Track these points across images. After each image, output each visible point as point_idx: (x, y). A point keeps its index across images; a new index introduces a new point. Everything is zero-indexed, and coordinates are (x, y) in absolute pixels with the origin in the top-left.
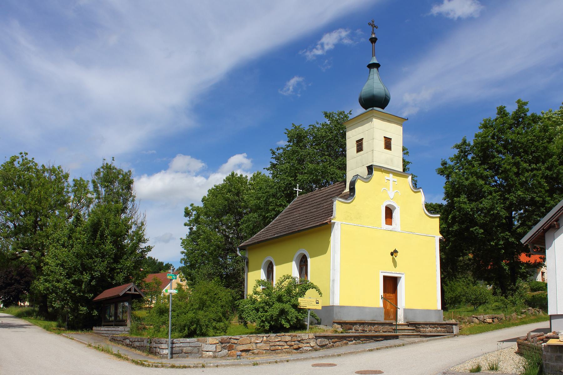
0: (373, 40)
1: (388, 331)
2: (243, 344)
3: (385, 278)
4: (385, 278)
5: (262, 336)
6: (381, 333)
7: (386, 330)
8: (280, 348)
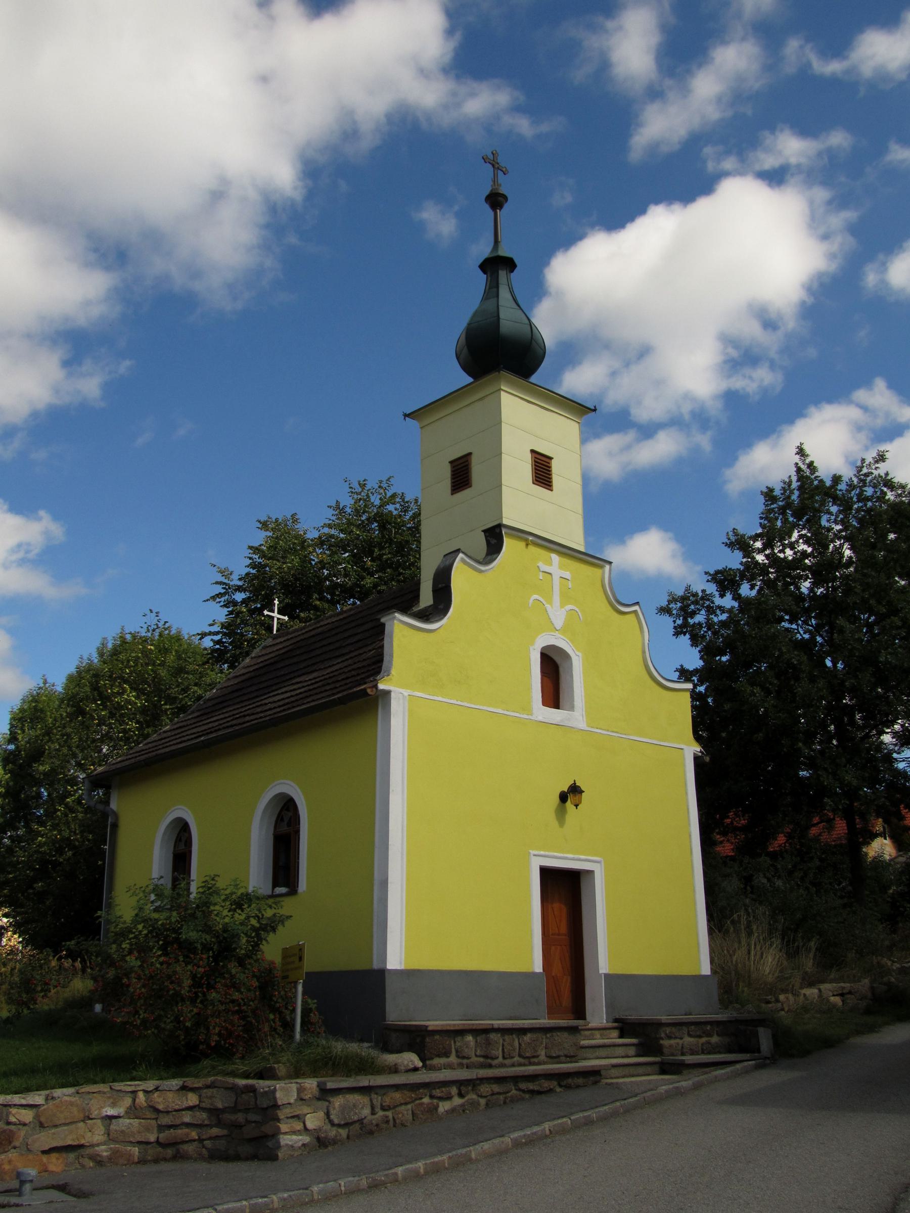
0: (496, 200)
1: (566, 1056)
2: (56, 1126)
3: (547, 874)
4: (547, 874)
5: (130, 1089)
6: (545, 1063)
7: (558, 1053)
8: (194, 1135)
